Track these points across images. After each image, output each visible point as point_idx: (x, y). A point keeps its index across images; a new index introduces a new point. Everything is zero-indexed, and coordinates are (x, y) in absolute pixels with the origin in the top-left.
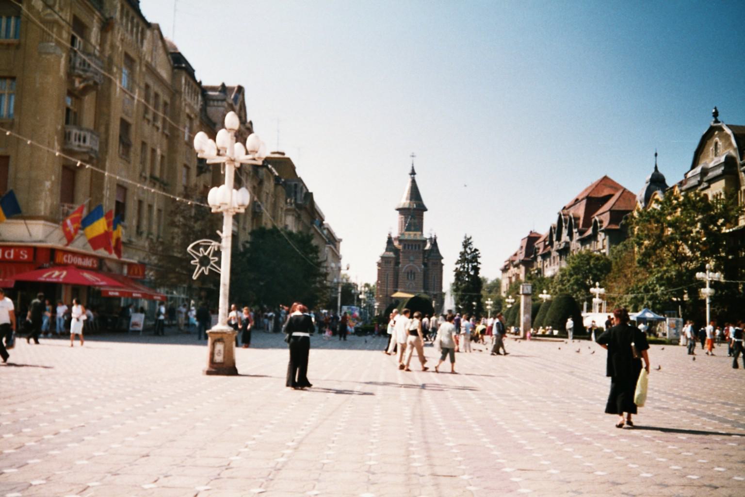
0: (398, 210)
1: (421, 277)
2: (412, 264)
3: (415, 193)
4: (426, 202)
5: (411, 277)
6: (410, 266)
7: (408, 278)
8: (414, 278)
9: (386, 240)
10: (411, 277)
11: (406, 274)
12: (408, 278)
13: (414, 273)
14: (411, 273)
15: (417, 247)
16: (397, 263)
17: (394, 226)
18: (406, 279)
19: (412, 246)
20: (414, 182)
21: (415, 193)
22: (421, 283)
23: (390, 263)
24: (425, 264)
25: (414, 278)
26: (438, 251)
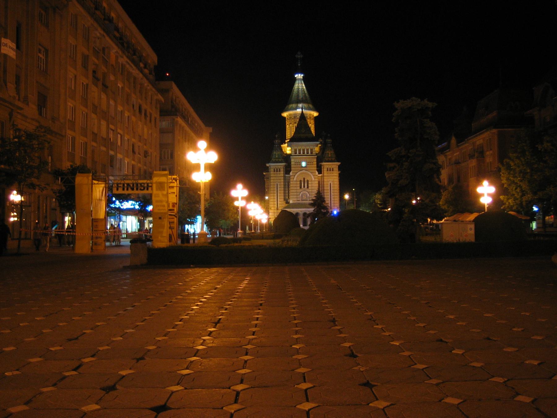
5: (304, 187)
6: (303, 173)
7: (301, 188)
8: (308, 187)
10: (304, 187)
11: (299, 183)
12: (301, 188)
13: (308, 181)
18: (299, 188)
23: (280, 171)
25: (308, 187)
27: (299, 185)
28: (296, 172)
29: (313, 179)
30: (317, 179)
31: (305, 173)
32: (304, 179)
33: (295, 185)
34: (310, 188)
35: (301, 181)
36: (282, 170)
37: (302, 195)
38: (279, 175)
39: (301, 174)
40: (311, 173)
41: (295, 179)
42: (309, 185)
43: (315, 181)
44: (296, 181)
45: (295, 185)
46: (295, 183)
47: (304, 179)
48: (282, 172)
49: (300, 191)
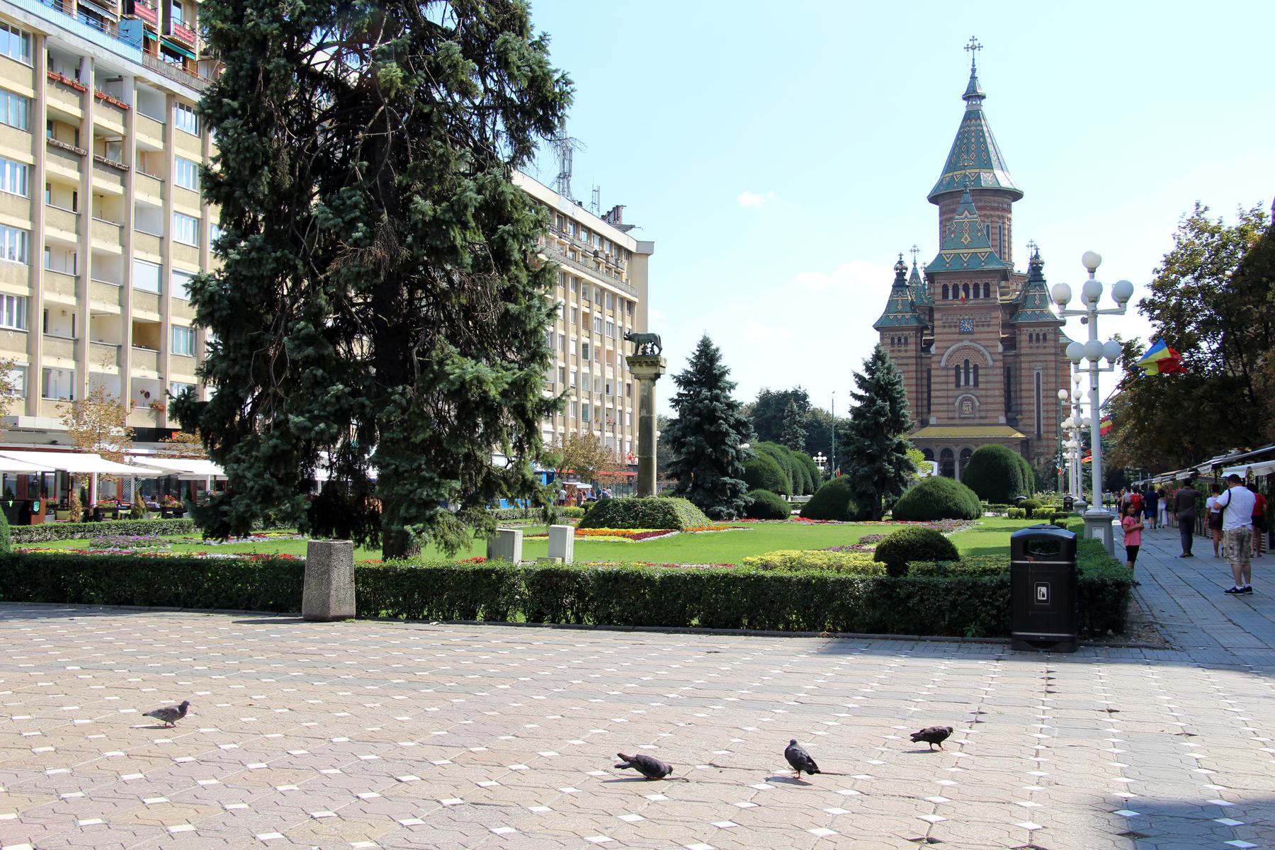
1: (997, 377)
2: (969, 340)
5: (967, 382)
6: (965, 348)
7: (958, 385)
8: (976, 384)
9: (893, 276)
10: (967, 382)
11: (953, 372)
12: (958, 385)
13: (976, 368)
14: (966, 372)
15: (982, 292)
18: (953, 386)
19: (966, 288)
20: (973, 117)
22: (998, 392)
23: (906, 343)
24: (1010, 344)
25: (976, 384)
27: (953, 379)
28: (945, 344)
29: (991, 363)
30: (1000, 364)
32: (967, 362)
33: (944, 379)
34: (981, 386)
35: (958, 368)
36: (912, 340)
37: (961, 404)
38: (903, 354)
39: (958, 349)
40: (985, 347)
41: (943, 364)
42: (980, 379)
43: (992, 368)
44: (946, 368)
45: (944, 379)
46: (945, 373)
47: (967, 362)
48: (912, 347)
49: (957, 393)
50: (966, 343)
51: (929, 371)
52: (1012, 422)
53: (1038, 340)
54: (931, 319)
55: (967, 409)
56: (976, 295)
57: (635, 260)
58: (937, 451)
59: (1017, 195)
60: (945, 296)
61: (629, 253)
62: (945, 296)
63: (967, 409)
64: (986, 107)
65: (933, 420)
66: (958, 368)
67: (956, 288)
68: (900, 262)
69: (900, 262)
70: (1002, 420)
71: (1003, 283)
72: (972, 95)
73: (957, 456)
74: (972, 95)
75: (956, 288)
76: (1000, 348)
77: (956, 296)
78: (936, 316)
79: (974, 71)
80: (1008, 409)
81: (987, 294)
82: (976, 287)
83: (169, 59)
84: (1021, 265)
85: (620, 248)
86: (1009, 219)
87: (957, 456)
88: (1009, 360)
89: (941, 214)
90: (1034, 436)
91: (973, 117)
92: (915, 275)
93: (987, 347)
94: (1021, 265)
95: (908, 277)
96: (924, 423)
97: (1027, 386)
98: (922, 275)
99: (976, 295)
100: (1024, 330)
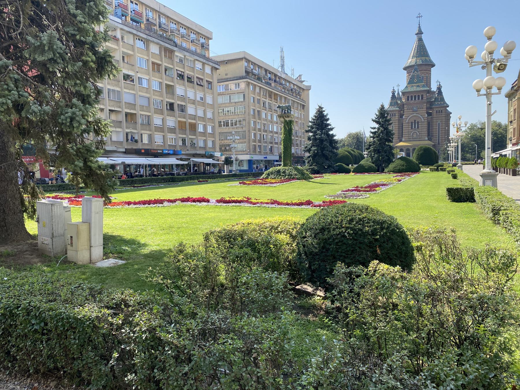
0: (405, 69)
1: (425, 125)
3: (421, 51)
4: (433, 57)
5: (415, 127)
6: (414, 116)
7: (412, 128)
8: (418, 127)
10: (415, 127)
12: (412, 128)
13: (418, 122)
14: (415, 124)
16: (401, 116)
17: (401, 82)
20: (420, 40)
21: (421, 51)
23: (395, 115)
24: (429, 114)
25: (418, 127)
26: (443, 99)
31: (416, 116)
32: (415, 121)
35: (412, 123)
37: (413, 134)
44: (408, 123)
47: (415, 121)
48: (397, 117)
50: (415, 114)
51: (402, 124)
52: (430, 139)
53: (439, 112)
54: (403, 108)
55: (415, 136)
56: (419, 99)
57: (305, 92)
58: (404, 149)
59: (433, 65)
60: (408, 100)
61: (303, 89)
62: (408, 100)
63: (415, 136)
64: (423, 36)
65: (403, 140)
66: (412, 123)
67: (412, 97)
68: (394, 90)
69: (394, 90)
70: (427, 139)
71: (428, 95)
72: (420, 33)
73: (411, 151)
74: (420, 33)
75: (412, 97)
76: (426, 115)
77: (412, 99)
78: (405, 106)
79: (419, 25)
80: (428, 135)
81: (422, 98)
82: (419, 96)
83: (135, 24)
84: (434, 88)
85: (300, 88)
86: (430, 74)
87: (411, 151)
88: (429, 119)
89: (408, 73)
90: (437, 143)
91: (420, 40)
92: (398, 94)
93: (422, 116)
94: (434, 88)
95: (396, 94)
96: (401, 141)
97: (435, 128)
98: (401, 94)
99: (419, 99)
100: (435, 109)
